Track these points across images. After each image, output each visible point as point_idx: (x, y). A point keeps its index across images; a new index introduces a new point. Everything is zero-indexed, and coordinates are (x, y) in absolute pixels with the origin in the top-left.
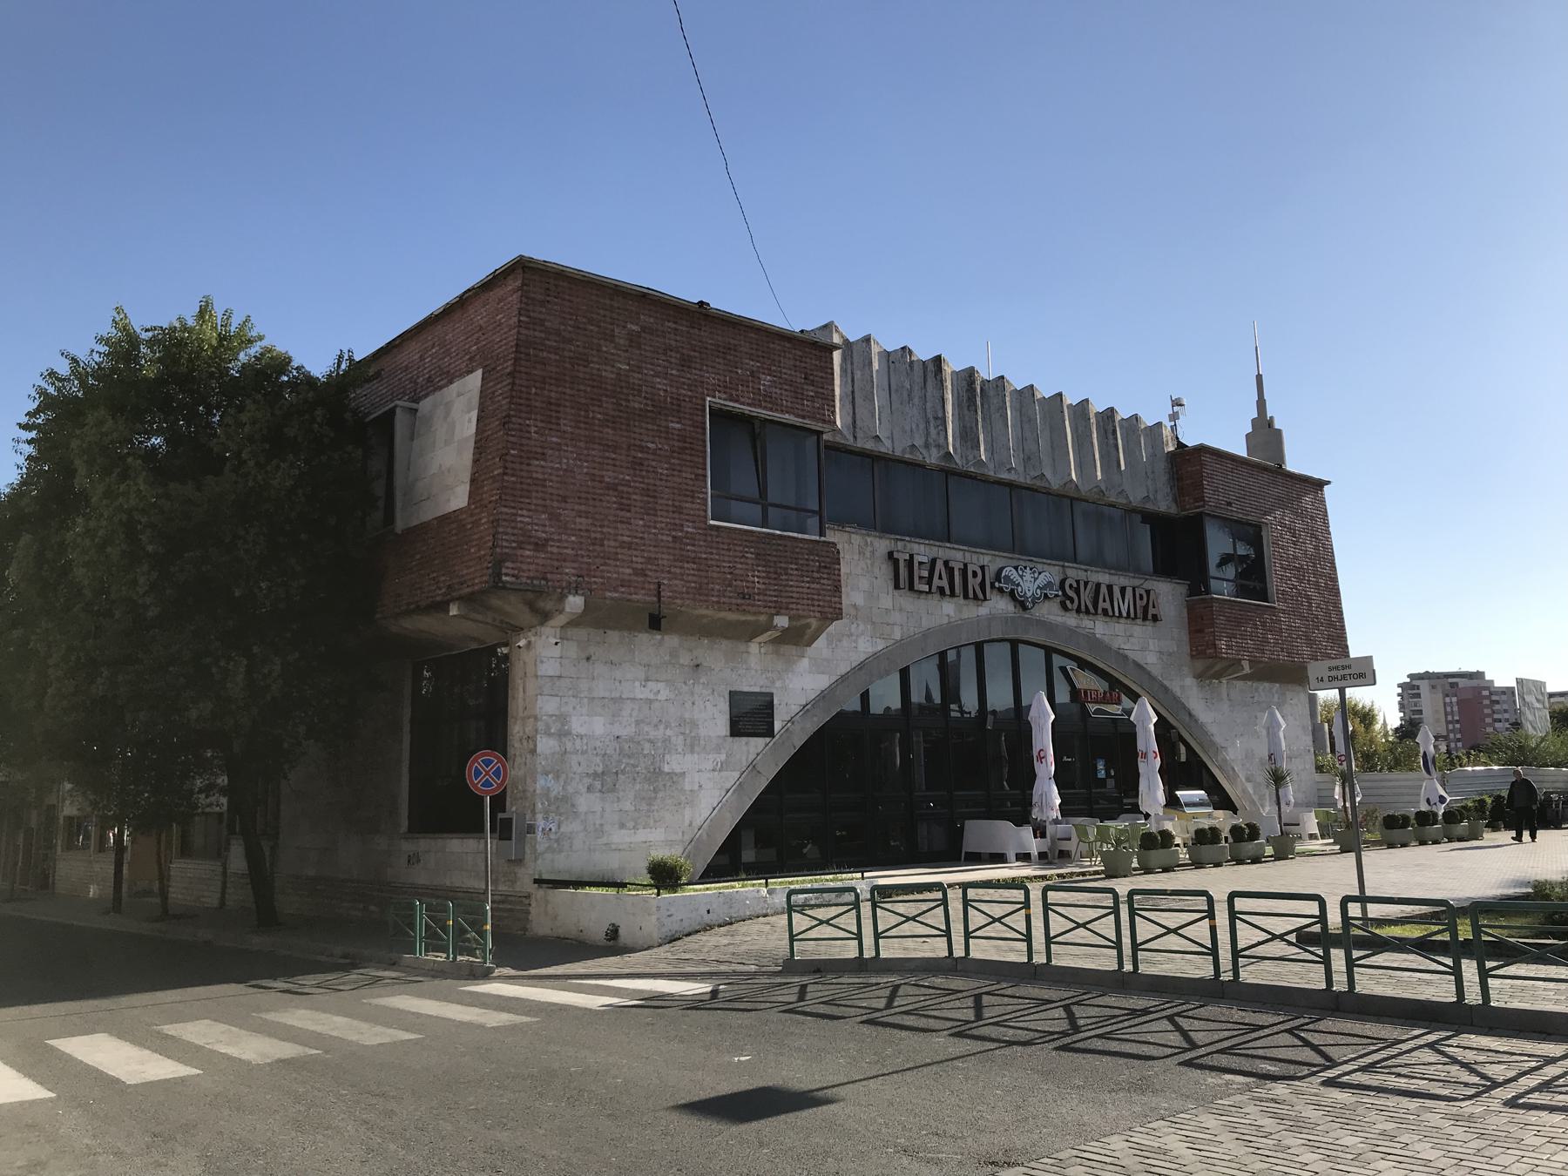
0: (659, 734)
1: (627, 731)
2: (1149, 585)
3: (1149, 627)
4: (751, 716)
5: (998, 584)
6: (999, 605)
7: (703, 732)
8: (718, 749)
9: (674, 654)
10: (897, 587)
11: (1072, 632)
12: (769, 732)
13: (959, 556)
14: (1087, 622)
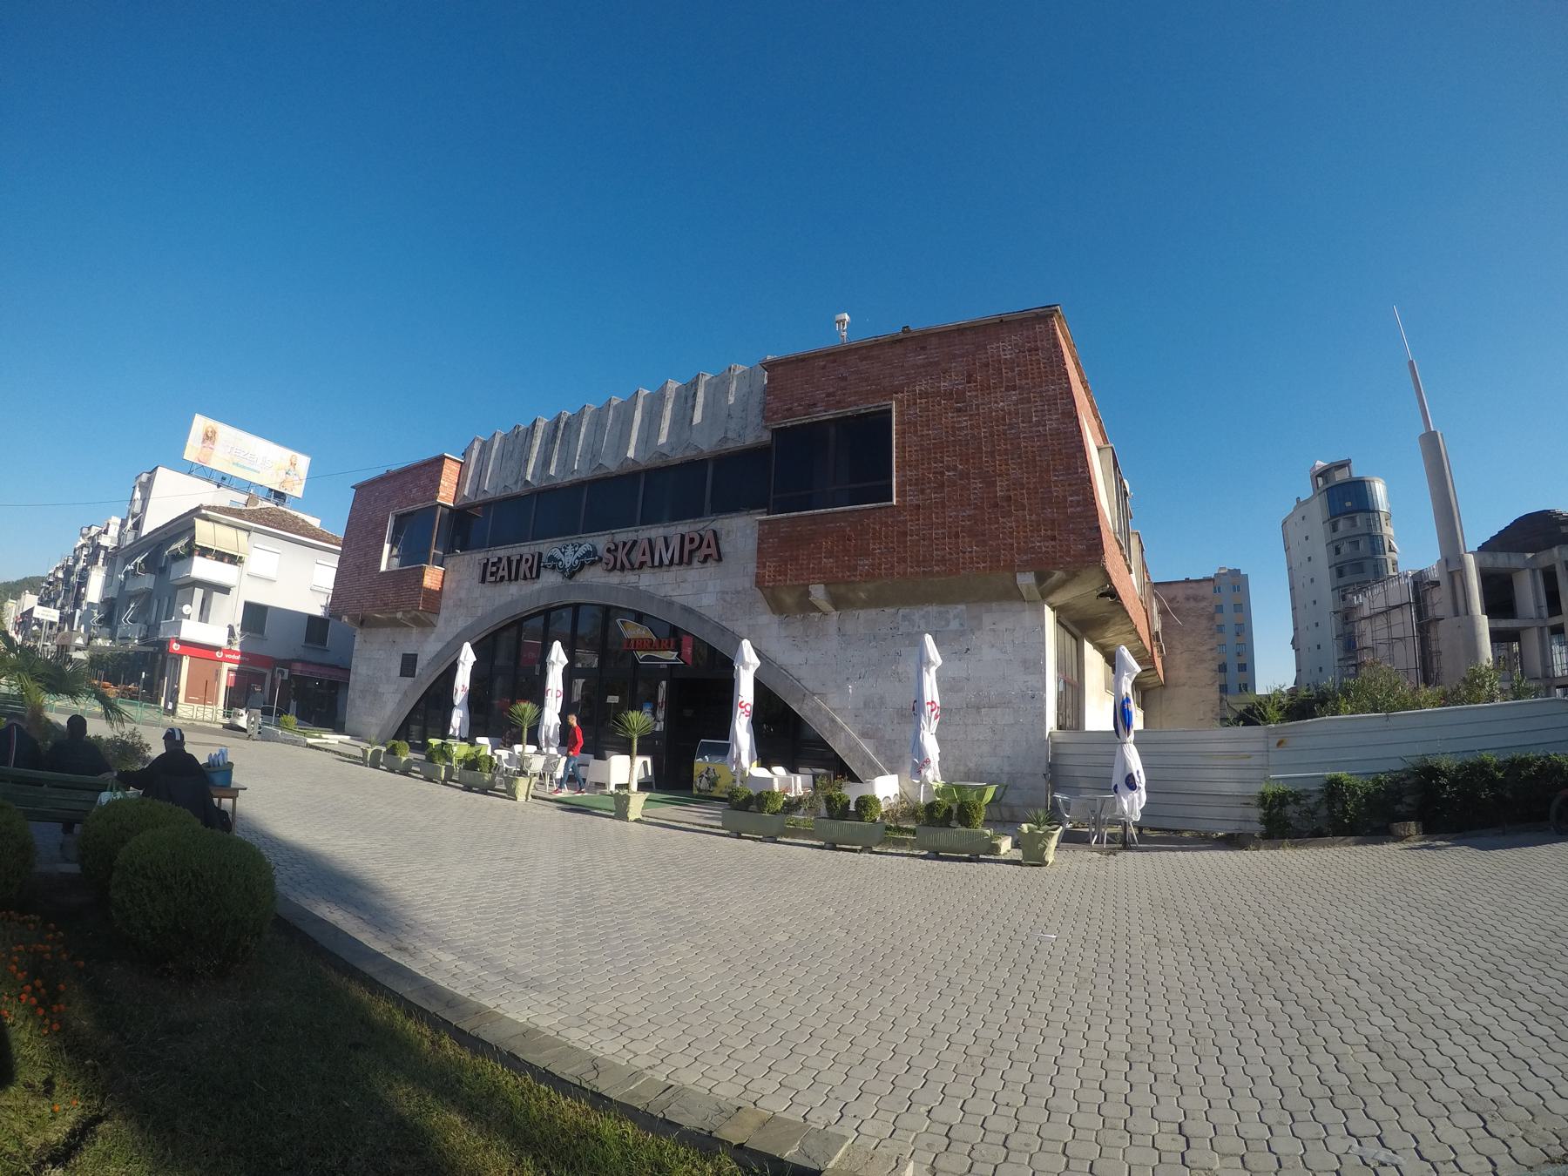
2: (713, 526)
3: (711, 566)
5: (537, 567)
6: (550, 579)
10: (483, 580)
13: (514, 551)
14: (631, 578)
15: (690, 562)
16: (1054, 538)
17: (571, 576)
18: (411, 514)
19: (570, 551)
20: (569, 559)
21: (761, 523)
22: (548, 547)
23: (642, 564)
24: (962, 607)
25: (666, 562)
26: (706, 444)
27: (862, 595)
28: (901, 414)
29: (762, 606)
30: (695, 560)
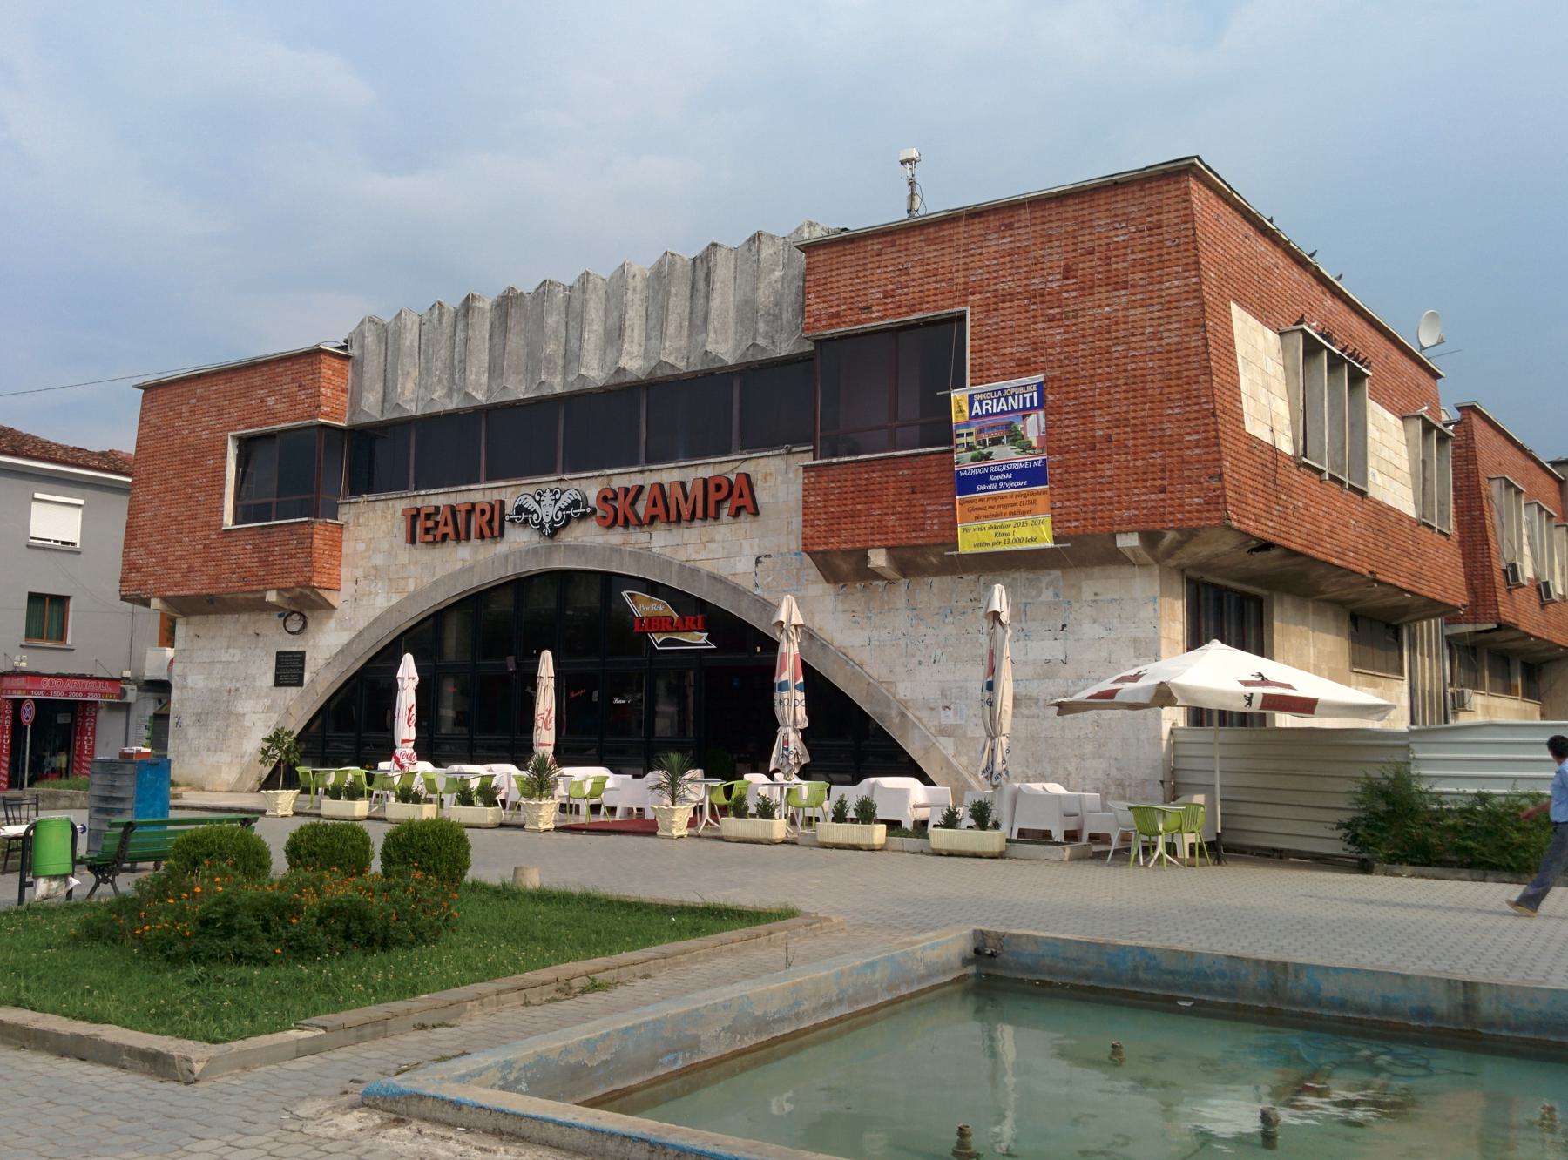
0: (232, 686)
1: (214, 685)
4: (289, 670)
6: (519, 538)
7: (258, 683)
8: (267, 696)
9: (245, 628)
10: (412, 540)
11: (614, 550)
12: (300, 683)
14: (638, 537)
15: (717, 517)
16: (1163, 490)
17: (554, 532)
18: (269, 436)
19: (548, 499)
20: (548, 511)
21: (806, 468)
22: (510, 494)
23: (653, 519)
24: (1057, 573)
25: (686, 513)
26: (725, 348)
27: (934, 560)
28: (978, 324)
29: (812, 571)
30: (725, 512)
